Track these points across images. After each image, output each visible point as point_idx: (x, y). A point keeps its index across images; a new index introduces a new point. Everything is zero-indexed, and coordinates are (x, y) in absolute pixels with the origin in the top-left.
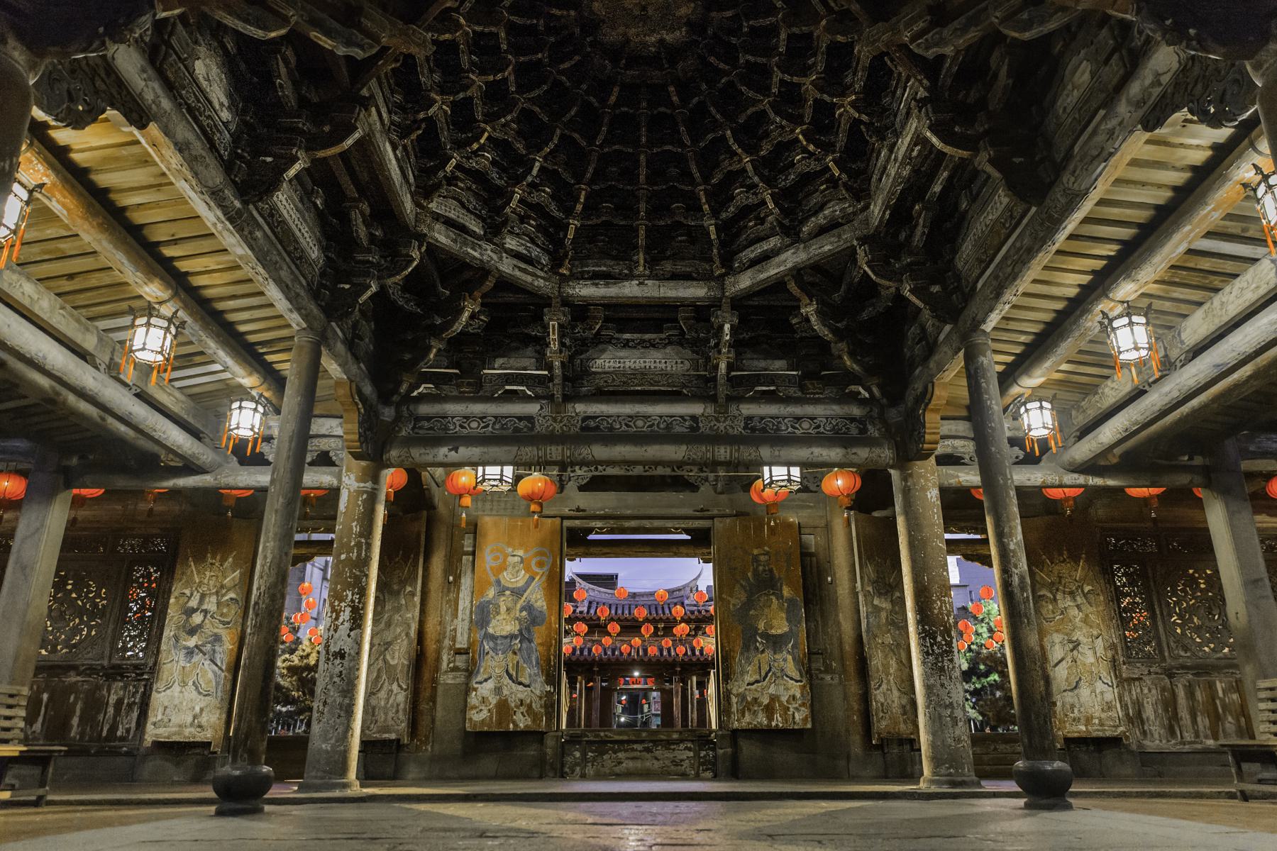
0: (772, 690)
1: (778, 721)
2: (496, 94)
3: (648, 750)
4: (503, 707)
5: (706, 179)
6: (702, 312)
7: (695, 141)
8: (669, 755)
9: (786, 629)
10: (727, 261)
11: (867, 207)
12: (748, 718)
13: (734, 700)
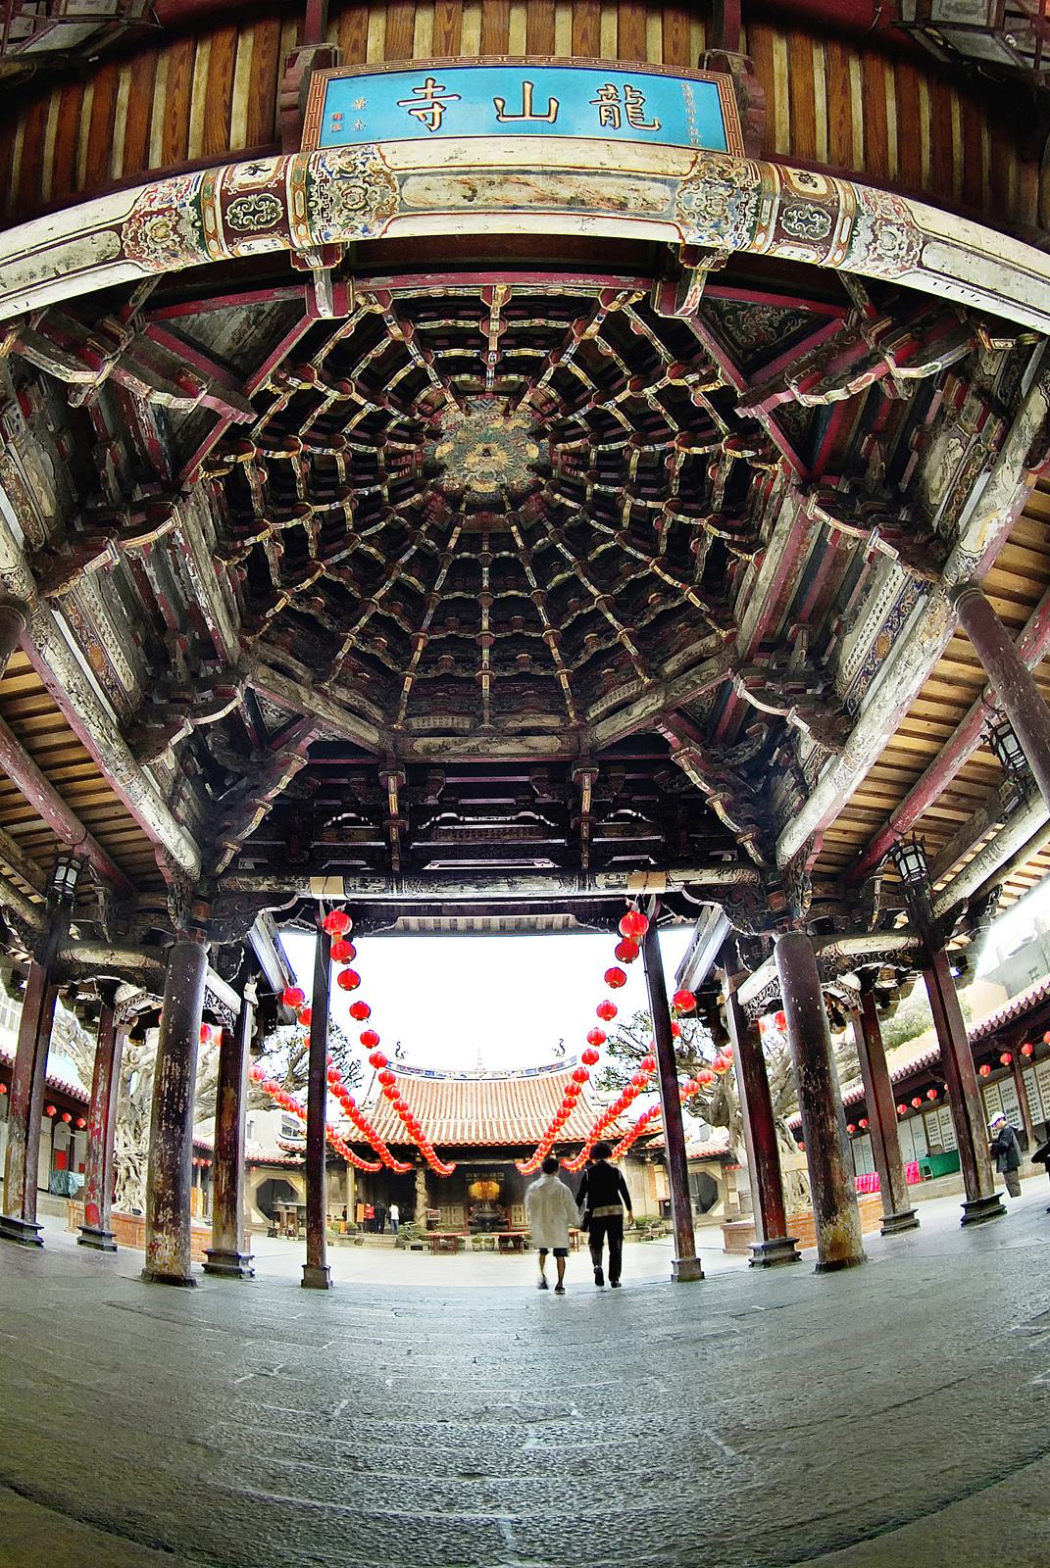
2: (333, 530)
5: (555, 623)
6: (556, 771)
7: (542, 584)
10: (581, 713)
11: (732, 637)
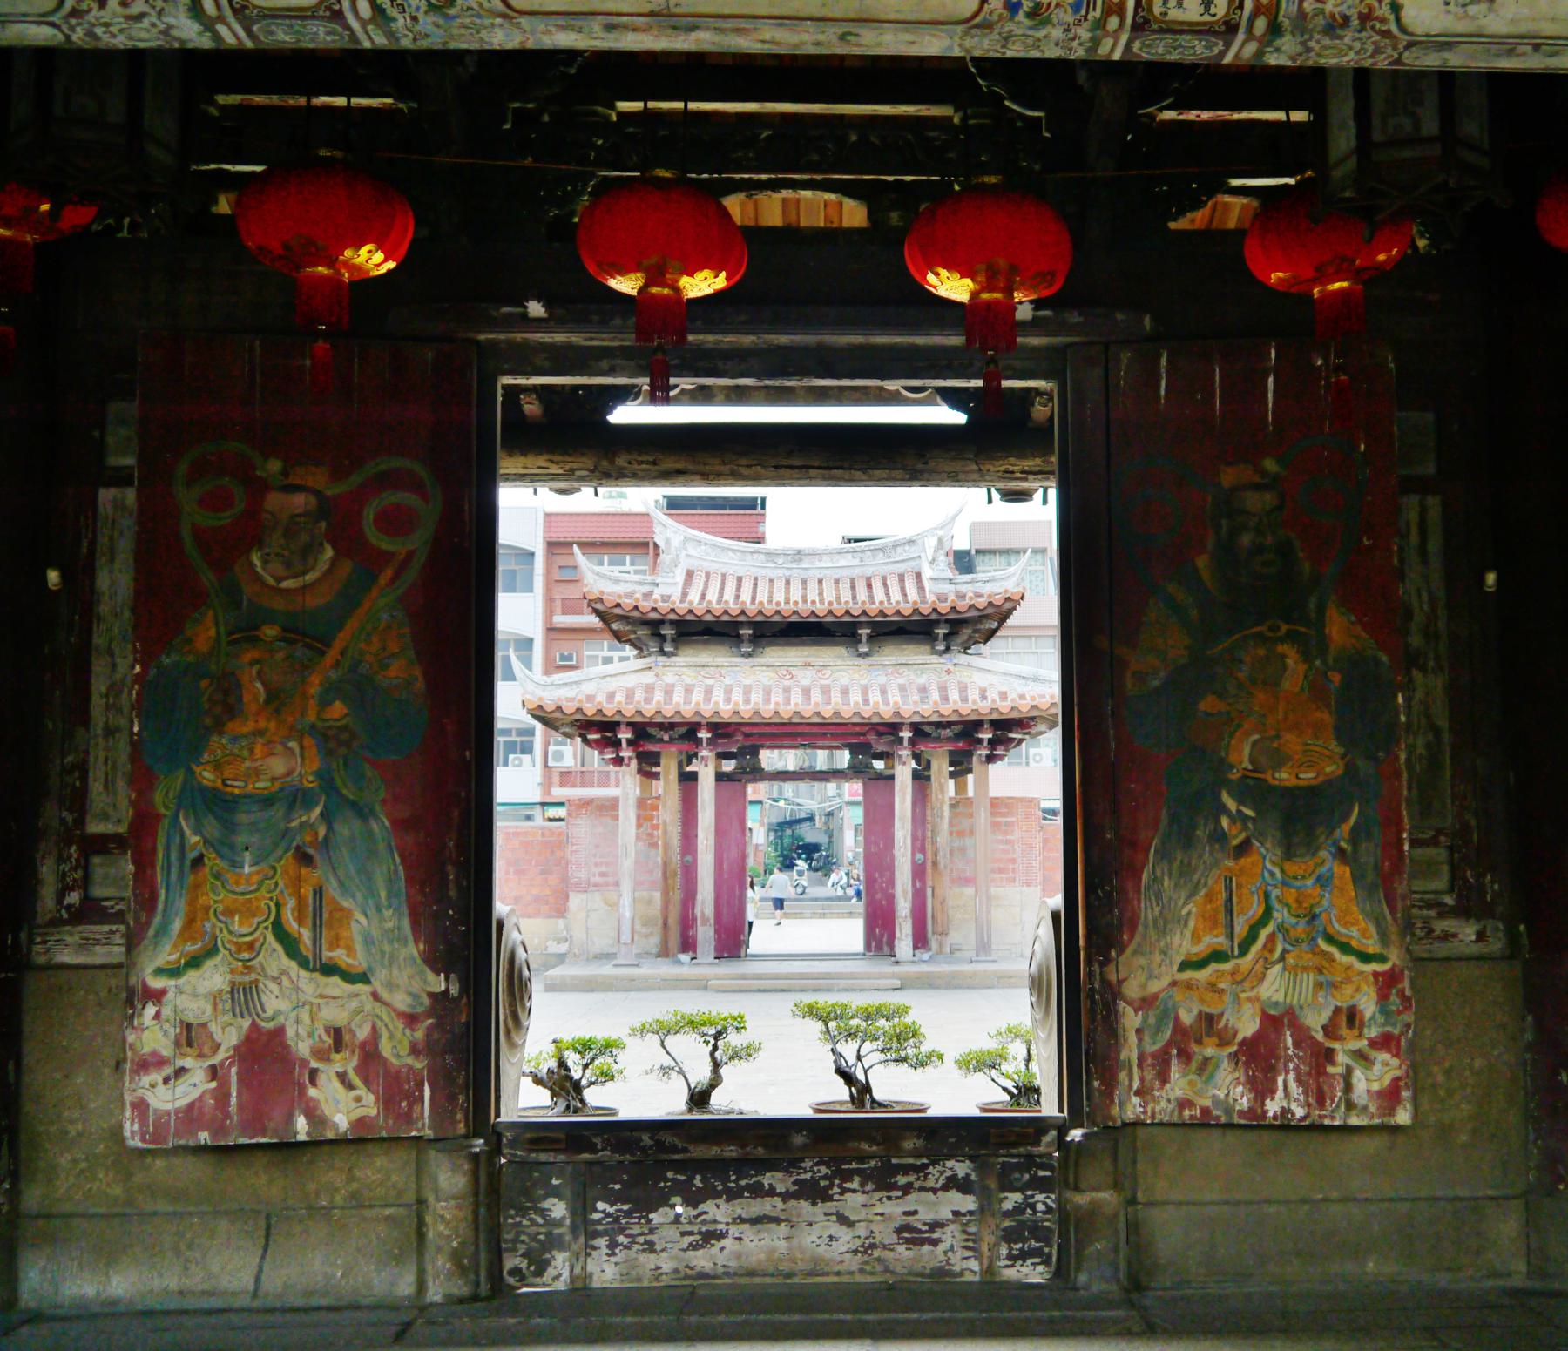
0: (1273, 988)
1: (1288, 1098)
3: (814, 1192)
4: (265, 1056)
8: (895, 1209)
9: (1332, 769)
12: (1179, 1083)
13: (1131, 1020)
